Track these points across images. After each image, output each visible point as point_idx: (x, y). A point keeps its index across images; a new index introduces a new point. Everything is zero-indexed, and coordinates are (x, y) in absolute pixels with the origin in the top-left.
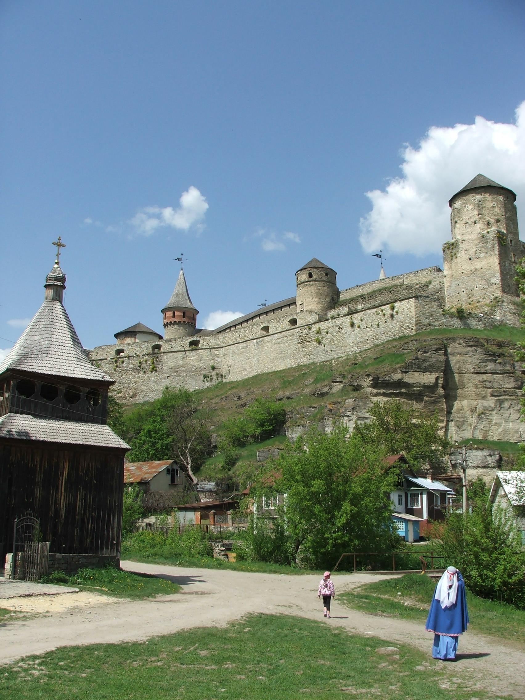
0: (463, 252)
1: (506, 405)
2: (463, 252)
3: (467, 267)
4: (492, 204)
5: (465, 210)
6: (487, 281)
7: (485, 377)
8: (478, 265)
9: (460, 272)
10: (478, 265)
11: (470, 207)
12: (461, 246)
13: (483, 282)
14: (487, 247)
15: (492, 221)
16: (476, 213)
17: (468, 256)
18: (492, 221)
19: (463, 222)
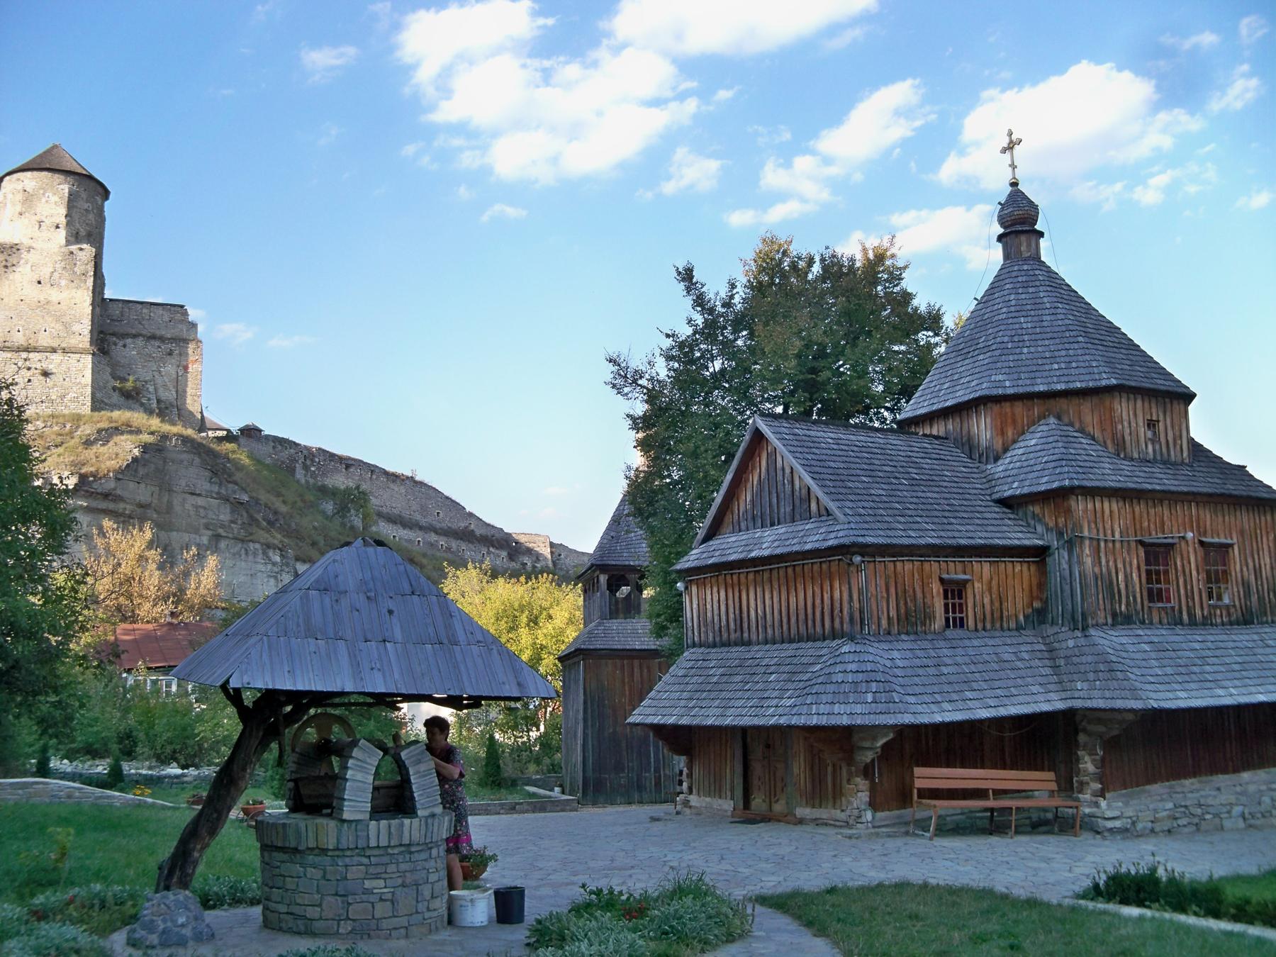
0: (29, 266)
1: (223, 544)
2: (29, 266)
3: (33, 293)
4: (86, 206)
5: (44, 200)
6: (66, 326)
7: (200, 501)
8: (54, 295)
9: (17, 297)
10: (54, 295)
11: (55, 198)
12: (24, 255)
13: (59, 326)
14: (74, 273)
15: (83, 233)
16: (63, 211)
17: (36, 278)
18: (83, 233)
19: (37, 218)
